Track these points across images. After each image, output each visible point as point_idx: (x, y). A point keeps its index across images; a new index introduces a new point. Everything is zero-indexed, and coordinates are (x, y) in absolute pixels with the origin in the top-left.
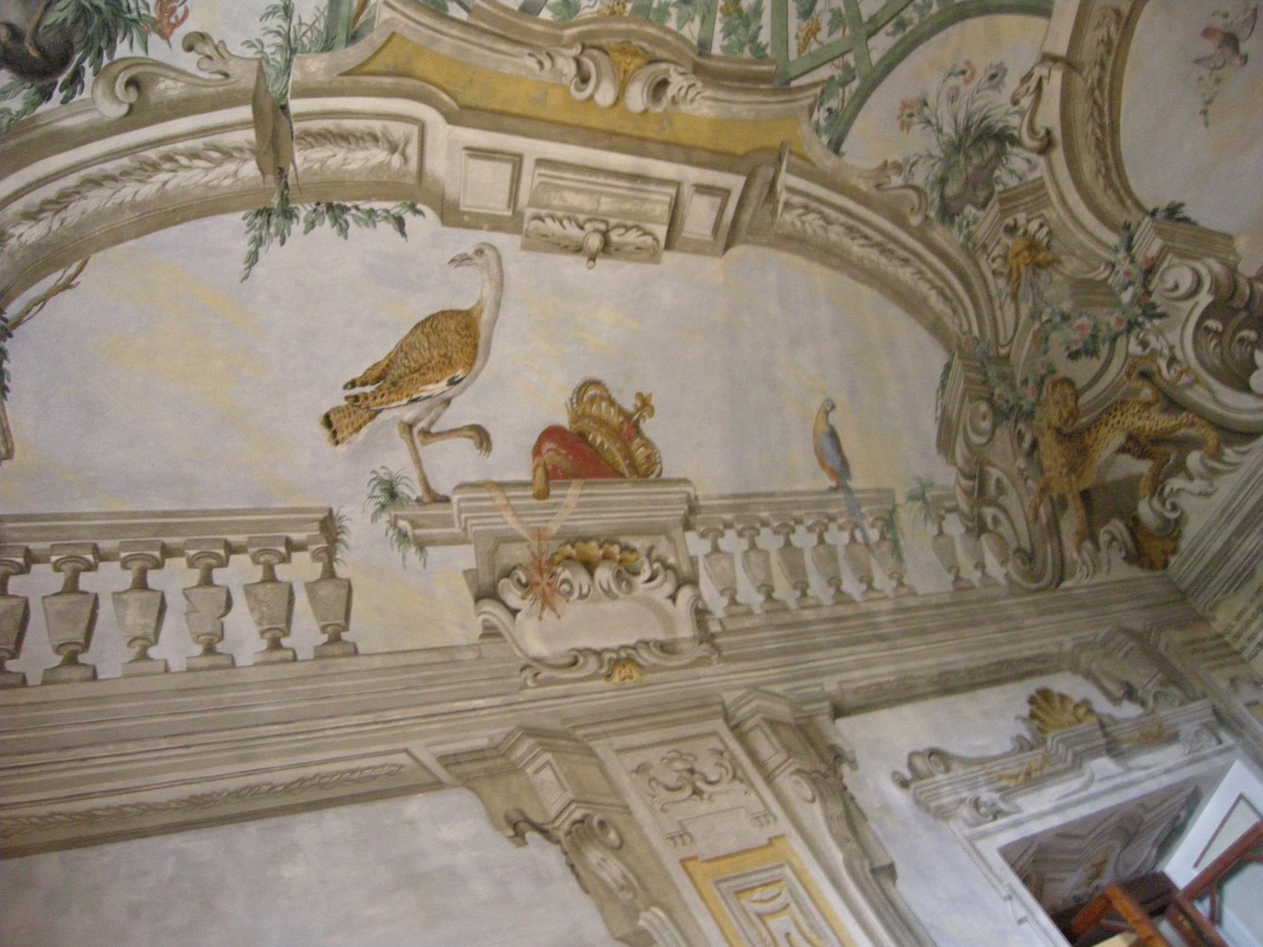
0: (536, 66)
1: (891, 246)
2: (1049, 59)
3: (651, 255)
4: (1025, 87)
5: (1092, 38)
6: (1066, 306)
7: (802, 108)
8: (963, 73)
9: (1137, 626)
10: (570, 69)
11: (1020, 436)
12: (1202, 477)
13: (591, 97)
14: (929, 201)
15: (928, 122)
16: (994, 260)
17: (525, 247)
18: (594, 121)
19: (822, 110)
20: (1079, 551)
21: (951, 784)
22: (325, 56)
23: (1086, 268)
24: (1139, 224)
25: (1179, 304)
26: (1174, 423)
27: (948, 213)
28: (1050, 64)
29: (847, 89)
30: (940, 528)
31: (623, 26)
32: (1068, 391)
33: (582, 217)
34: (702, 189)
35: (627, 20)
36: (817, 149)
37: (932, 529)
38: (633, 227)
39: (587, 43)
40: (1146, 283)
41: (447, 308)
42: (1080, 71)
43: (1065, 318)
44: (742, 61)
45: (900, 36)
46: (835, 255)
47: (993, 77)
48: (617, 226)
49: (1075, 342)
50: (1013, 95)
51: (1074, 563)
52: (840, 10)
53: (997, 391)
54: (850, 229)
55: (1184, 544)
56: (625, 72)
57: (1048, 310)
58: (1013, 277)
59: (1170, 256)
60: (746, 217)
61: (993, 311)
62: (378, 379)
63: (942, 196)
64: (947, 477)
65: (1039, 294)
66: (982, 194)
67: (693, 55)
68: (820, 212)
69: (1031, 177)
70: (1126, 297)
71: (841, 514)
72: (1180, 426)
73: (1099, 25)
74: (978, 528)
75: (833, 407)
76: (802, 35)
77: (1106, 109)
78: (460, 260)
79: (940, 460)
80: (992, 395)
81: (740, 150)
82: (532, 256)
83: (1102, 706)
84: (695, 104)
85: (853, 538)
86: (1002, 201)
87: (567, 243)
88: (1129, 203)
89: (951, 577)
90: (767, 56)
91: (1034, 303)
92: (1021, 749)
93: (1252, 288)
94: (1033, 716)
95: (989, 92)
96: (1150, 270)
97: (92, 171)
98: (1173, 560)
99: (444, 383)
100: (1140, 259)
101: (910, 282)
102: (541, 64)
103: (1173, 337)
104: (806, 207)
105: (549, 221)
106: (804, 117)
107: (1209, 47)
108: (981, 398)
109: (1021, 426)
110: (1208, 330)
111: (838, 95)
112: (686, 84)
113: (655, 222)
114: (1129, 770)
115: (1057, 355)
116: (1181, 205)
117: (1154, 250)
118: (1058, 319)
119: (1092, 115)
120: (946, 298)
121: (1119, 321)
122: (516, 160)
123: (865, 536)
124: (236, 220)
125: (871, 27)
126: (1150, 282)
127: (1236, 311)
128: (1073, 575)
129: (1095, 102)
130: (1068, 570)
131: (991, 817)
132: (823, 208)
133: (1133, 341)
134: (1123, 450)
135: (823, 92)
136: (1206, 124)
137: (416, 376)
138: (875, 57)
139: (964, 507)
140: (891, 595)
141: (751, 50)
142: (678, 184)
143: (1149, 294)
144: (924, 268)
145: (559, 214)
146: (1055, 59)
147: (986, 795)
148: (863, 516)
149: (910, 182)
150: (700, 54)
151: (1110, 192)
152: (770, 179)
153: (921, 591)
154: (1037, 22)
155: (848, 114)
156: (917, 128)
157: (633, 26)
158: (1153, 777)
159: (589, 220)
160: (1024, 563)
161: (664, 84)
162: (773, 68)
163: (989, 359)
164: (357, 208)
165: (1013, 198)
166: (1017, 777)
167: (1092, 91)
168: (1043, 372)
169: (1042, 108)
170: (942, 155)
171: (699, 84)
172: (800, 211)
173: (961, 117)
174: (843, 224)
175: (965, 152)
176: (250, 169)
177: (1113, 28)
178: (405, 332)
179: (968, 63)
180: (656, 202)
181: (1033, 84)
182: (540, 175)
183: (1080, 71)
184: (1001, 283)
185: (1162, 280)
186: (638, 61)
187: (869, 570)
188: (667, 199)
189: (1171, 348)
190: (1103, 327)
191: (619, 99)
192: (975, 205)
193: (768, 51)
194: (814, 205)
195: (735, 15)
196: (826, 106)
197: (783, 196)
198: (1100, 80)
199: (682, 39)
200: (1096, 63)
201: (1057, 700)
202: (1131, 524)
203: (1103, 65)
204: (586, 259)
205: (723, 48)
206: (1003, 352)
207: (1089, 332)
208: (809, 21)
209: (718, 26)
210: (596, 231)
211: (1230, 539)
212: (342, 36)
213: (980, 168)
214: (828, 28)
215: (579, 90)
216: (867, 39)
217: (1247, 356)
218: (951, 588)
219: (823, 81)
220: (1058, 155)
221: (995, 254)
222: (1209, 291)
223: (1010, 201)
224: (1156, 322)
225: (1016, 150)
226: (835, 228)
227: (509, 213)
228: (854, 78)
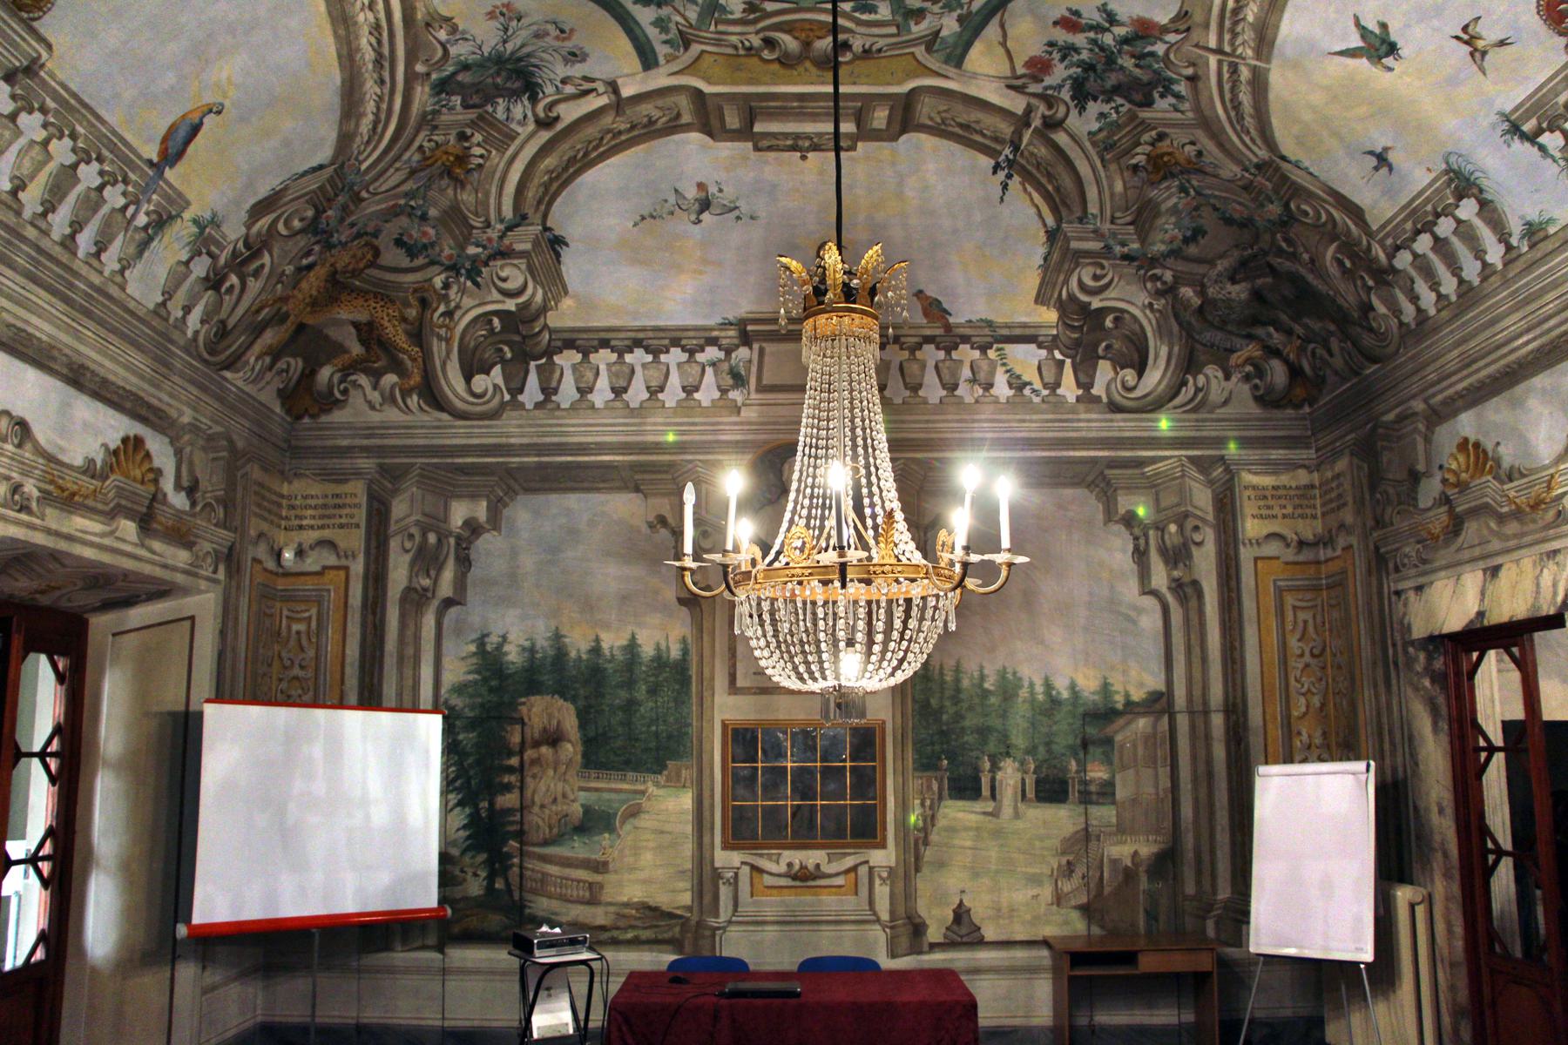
1: (386, 64)
2: (613, 87)
5: (647, 109)
6: (433, 212)
8: (562, 31)
9: (240, 444)
11: (309, 253)
12: (382, 395)
15: (506, 30)
16: (430, 141)
20: (257, 359)
21: (12, 459)
23: (472, 208)
24: (532, 224)
25: (494, 290)
26: (405, 346)
27: (443, 87)
28: (610, 89)
30: (191, 259)
32: (369, 256)
37: (184, 257)
40: (493, 257)
42: (618, 114)
43: (424, 218)
46: (347, 29)
47: (574, 54)
49: (411, 236)
50: (568, 77)
51: (247, 362)
53: (330, 213)
54: (377, 27)
55: (324, 419)
57: (421, 202)
58: (426, 161)
59: (525, 261)
61: (391, 166)
63: (454, 74)
64: (233, 231)
65: (428, 187)
66: (476, 100)
69: (514, 126)
70: (472, 250)
71: (136, 184)
72: (405, 352)
73: (660, 109)
74: (214, 282)
75: (219, 113)
77: (602, 149)
79: (244, 216)
80: (325, 211)
83: (168, 484)
85: (125, 207)
86: (481, 117)
88: (543, 207)
89: (160, 299)
91: (418, 188)
92: (84, 473)
93: (540, 332)
94: (116, 453)
96: (505, 254)
98: (306, 420)
100: (506, 241)
101: (368, 96)
103: (467, 302)
107: (691, 193)
108: (315, 206)
109: (317, 248)
110: (490, 322)
114: (143, 545)
115: (392, 229)
116: (567, 245)
117: (519, 247)
118: (419, 213)
119: (590, 142)
120: (374, 129)
121: (450, 257)
123: (134, 216)
126: (495, 259)
127: (518, 332)
128: (238, 371)
129: (602, 139)
130: (239, 365)
131: (17, 508)
133: (443, 276)
134: (356, 325)
136: (636, 225)
139: (222, 261)
140: (107, 273)
143: (486, 264)
144: (386, 99)
147: (30, 488)
148: (149, 201)
151: (542, 190)
153: (129, 291)
154: (636, 64)
156: (495, 24)
158: (153, 563)
160: (215, 335)
163: (351, 188)
165: (491, 125)
166: (63, 490)
167: (609, 131)
168: (369, 230)
170: (486, 54)
173: (525, 50)
174: (377, 19)
177: (664, 119)
181: (587, 86)
183: (618, 114)
184: (417, 157)
185: (502, 267)
187: (110, 241)
189: (458, 307)
190: (437, 249)
192: (463, 101)
198: (620, 133)
201: (143, 453)
202: (307, 372)
203: (633, 127)
206: (364, 194)
207: (425, 241)
211: (354, 447)
213: (496, 86)
217: (490, 361)
218: (151, 306)
220: (545, 136)
221: (435, 138)
222: (517, 305)
223: (484, 122)
224: (469, 283)
225: (526, 103)
226: (370, 16)
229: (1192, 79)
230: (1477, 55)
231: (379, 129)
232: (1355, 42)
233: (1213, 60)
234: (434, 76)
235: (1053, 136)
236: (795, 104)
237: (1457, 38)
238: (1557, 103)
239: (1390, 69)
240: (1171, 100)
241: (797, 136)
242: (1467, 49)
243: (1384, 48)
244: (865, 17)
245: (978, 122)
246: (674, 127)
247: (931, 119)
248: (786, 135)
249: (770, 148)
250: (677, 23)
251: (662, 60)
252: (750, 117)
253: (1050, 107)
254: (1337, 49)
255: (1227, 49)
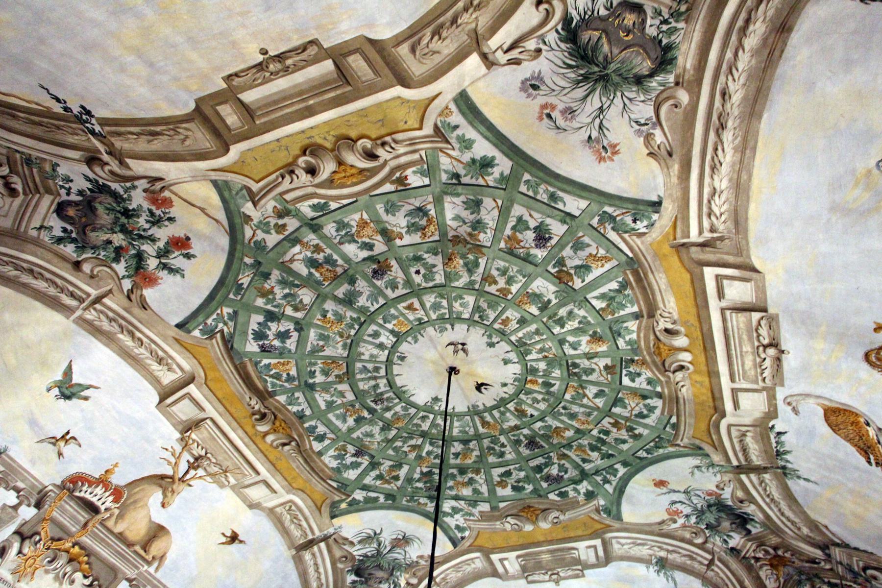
0: (685, 388)
2: (488, 61)
3: (773, 321)
4: (521, 57)
5: (447, 47)
7: (642, 243)
8: (549, 116)
10: (679, 375)
13: (690, 362)
14: (662, 88)
17: (783, 385)
18: (702, 359)
19: (637, 227)
22: (711, 455)
29: (615, 214)
31: (647, 358)
33: (758, 360)
34: (721, 295)
35: (644, 357)
36: (664, 219)
38: (757, 330)
39: (664, 369)
41: (823, 419)
42: (475, 31)
44: (635, 294)
45: (561, 194)
47: (535, 87)
48: (759, 341)
50: (535, 58)
52: (572, 247)
56: (670, 350)
60: (731, 259)
62: (866, 452)
67: (645, 320)
68: (709, 202)
73: (435, 52)
76: (600, 263)
78: (795, 411)
81: (687, 276)
82: (786, 383)
84: (671, 311)
87: (775, 366)
90: (623, 279)
95: (548, 81)
97: (778, 514)
99: (868, 428)
102: (682, 386)
104: (709, 216)
105: (764, 375)
106: (648, 239)
111: (622, 219)
112: (662, 320)
113: (751, 320)
120: (748, 21)
122: (734, 392)
124: (790, 483)
125: (568, 220)
132: (705, 201)
135: (626, 232)
137: (864, 438)
138: (583, 204)
141: (626, 289)
142: (723, 310)
144: (725, 67)
145: (759, 370)
146: (484, 57)
149: (654, 120)
150: (643, 316)
152: (699, 249)
155: (630, 206)
157: (645, 353)
159: (759, 356)
161: (667, 331)
162: (628, 272)
164: (776, 447)
169: (526, 27)
171: (659, 312)
172: (713, 218)
173: (580, 92)
175: (605, 68)
176: (767, 477)
178: (838, 437)
179: (540, 119)
180: (737, 321)
181: (514, 54)
182: (739, 380)
183: (475, 31)
186: (661, 346)
188: (734, 315)
191: (686, 350)
193: (620, 279)
194: (705, 210)
195: (611, 306)
196: (633, 225)
197: (707, 235)
198: (466, 10)
199: (639, 328)
200: (457, 27)
203: (454, 21)
204: (783, 355)
205: (632, 306)
208: (589, 264)
209: (622, 313)
210: (764, 351)
212: (701, 452)
214: (586, 249)
215: (688, 369)
216: (576, 217)
219: (618, 234)
225: (574, 13)
227: (765, 393)
228: (605, 212)
229: (77, 265)
230: (53, 440)
231: (743, 15)
232: (76, 379)
233: (94, 293)
234: (671, 78)
235: (81, 153)
236: (311, 102)
237: (68, 433)
238: (17, 481)
239: (49, 390)
240: (58, 232)
241: (287, 71)
242: (59, 437)
243: (67, 392)
244: (315, 201)
245: (149, 141)
246: (412, 34)
247: (186, 129)
248: (297, 68)
249: (304, 48)
250: (453, 149)
251: (452, 106)
252: (343, 74)
253: (112, 172)
254: (75, 368)
255: (98, 306)
